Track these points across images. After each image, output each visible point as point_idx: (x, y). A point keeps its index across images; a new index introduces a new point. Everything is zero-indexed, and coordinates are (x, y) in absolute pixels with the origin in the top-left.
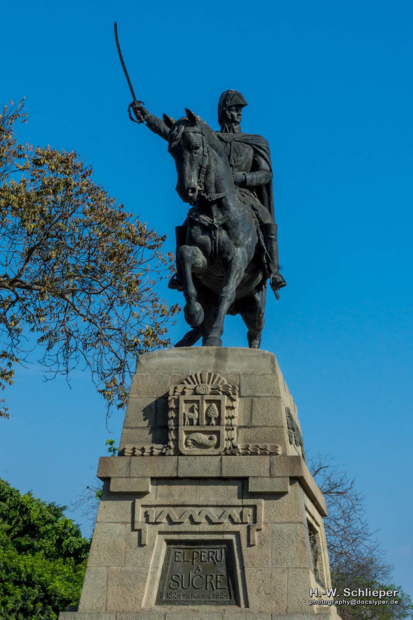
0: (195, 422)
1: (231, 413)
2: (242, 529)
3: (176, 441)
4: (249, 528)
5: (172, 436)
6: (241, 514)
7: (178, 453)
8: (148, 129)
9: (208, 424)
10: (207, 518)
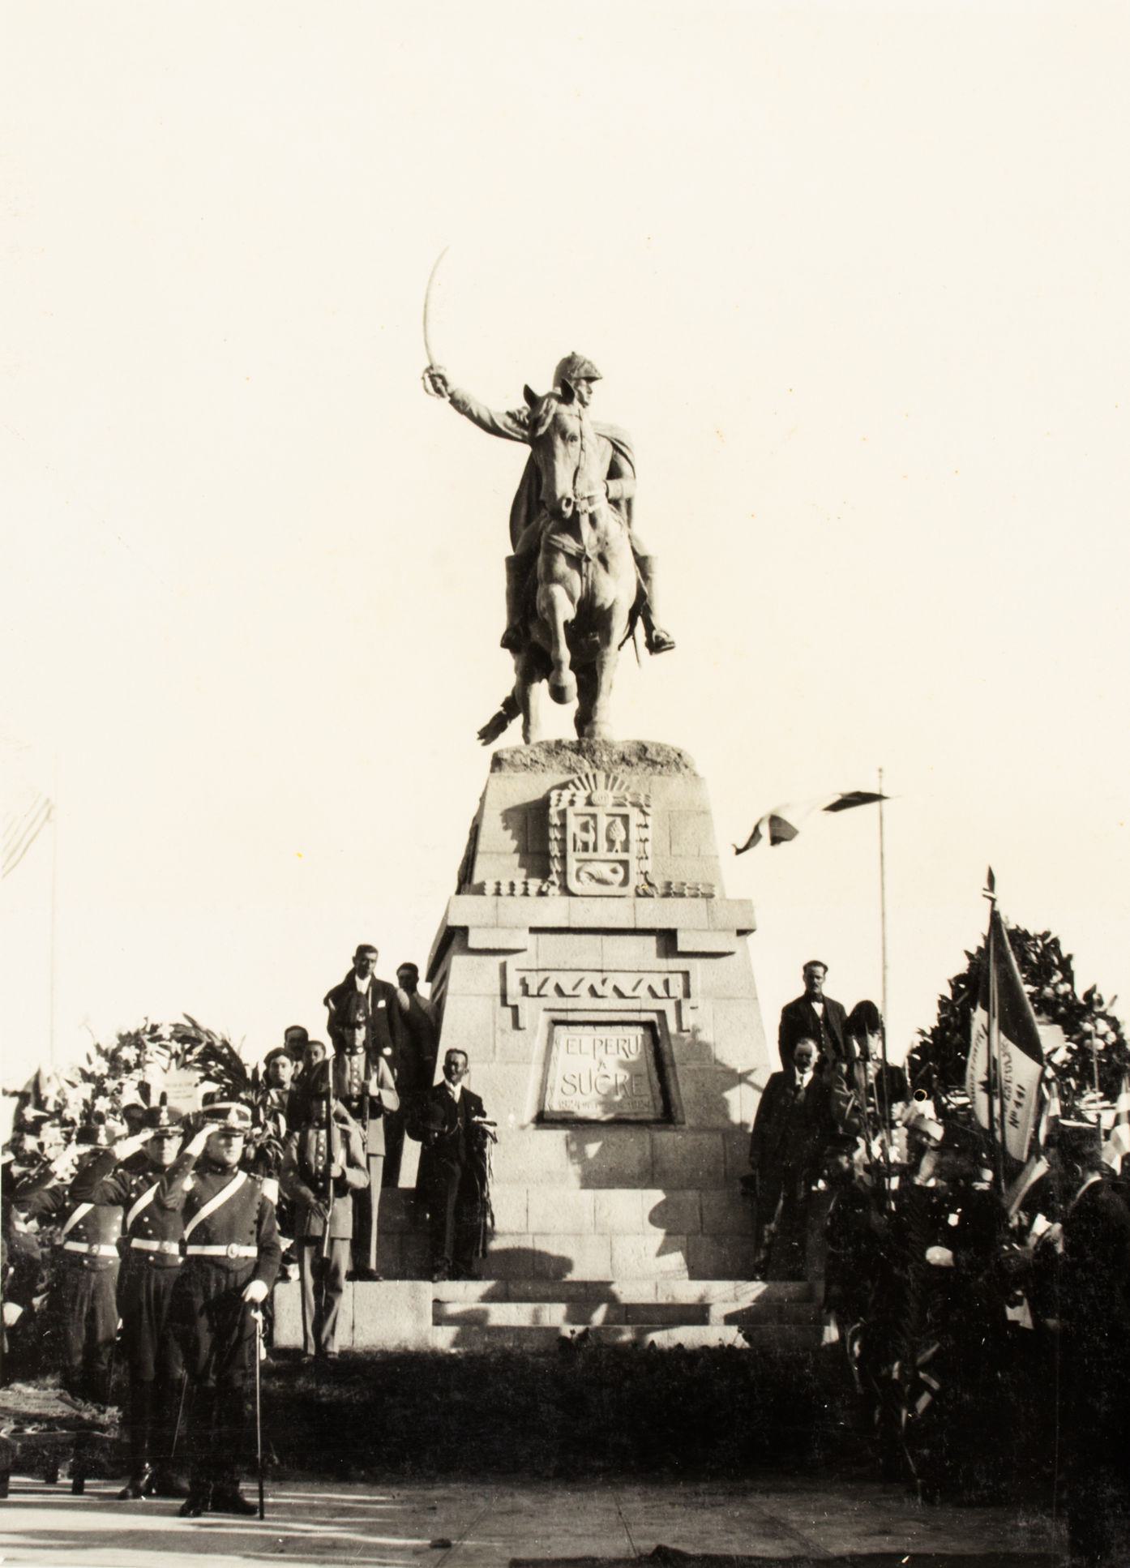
0: (591, 846)
1: (645, 833)
2: (669, 1006)
3: (563, 874)
4: (678, 1005)
5: (556, 866)
6: (666, 983)
7: (566, 891)
8: (451, 408)
9: (610, 850)
10: (616, 989)
